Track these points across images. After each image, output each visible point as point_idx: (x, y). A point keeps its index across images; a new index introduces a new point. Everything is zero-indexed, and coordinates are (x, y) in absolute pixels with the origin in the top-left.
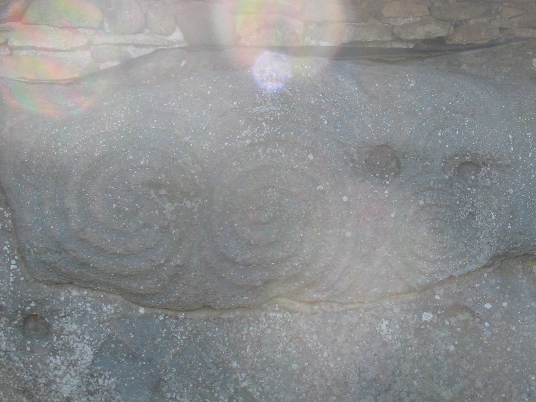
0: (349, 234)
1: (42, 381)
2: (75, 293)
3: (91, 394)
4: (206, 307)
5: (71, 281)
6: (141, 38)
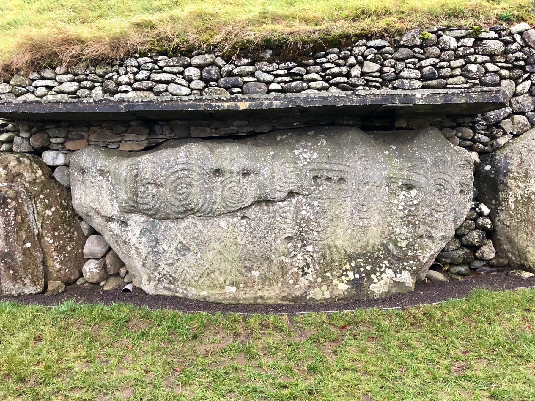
0: (208, 196)
1: (127, 240)
2: (133, 215)
3: (140, 243)
4: (169, 218)
5: (131, 212)
6: (161, 137)
